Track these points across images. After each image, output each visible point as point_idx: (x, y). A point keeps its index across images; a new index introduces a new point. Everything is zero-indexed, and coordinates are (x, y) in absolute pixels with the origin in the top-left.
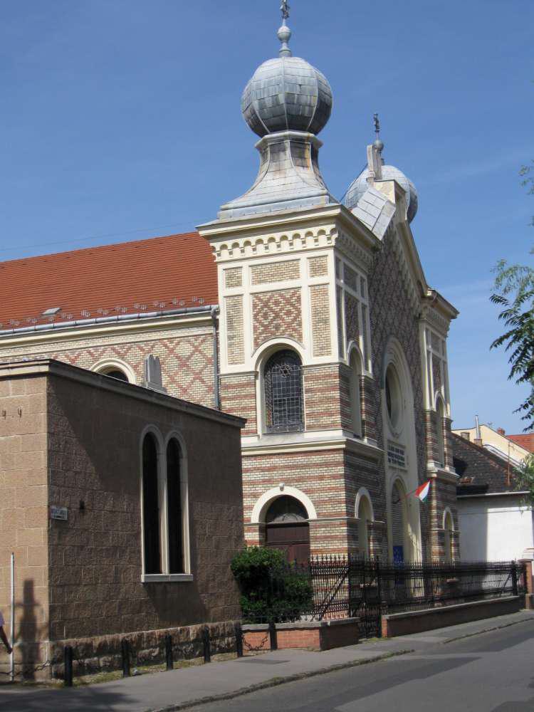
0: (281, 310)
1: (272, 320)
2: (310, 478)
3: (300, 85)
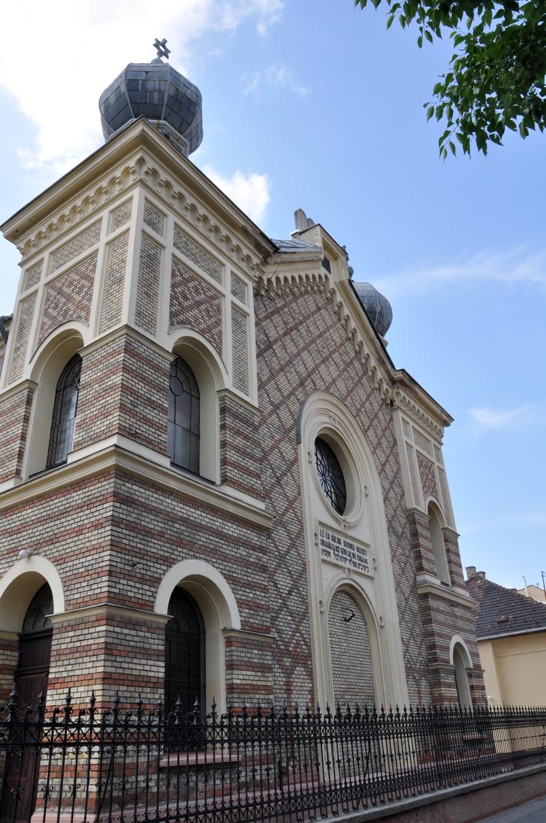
3: (147, 72)
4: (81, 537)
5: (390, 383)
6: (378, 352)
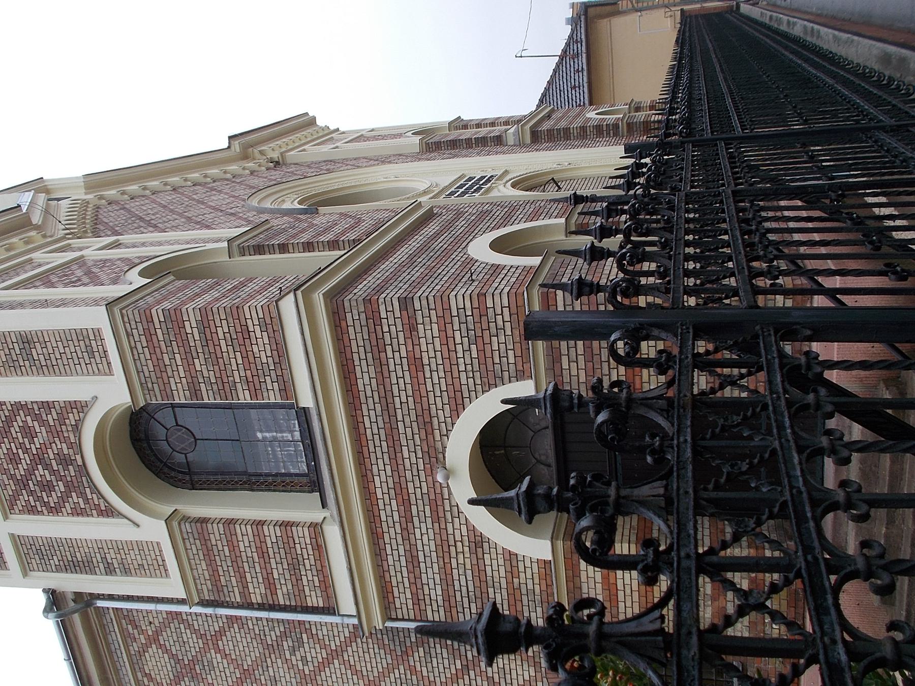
0: (26, 451)
1: (53, 472)
2: (419, 395)
4: (426, 361)
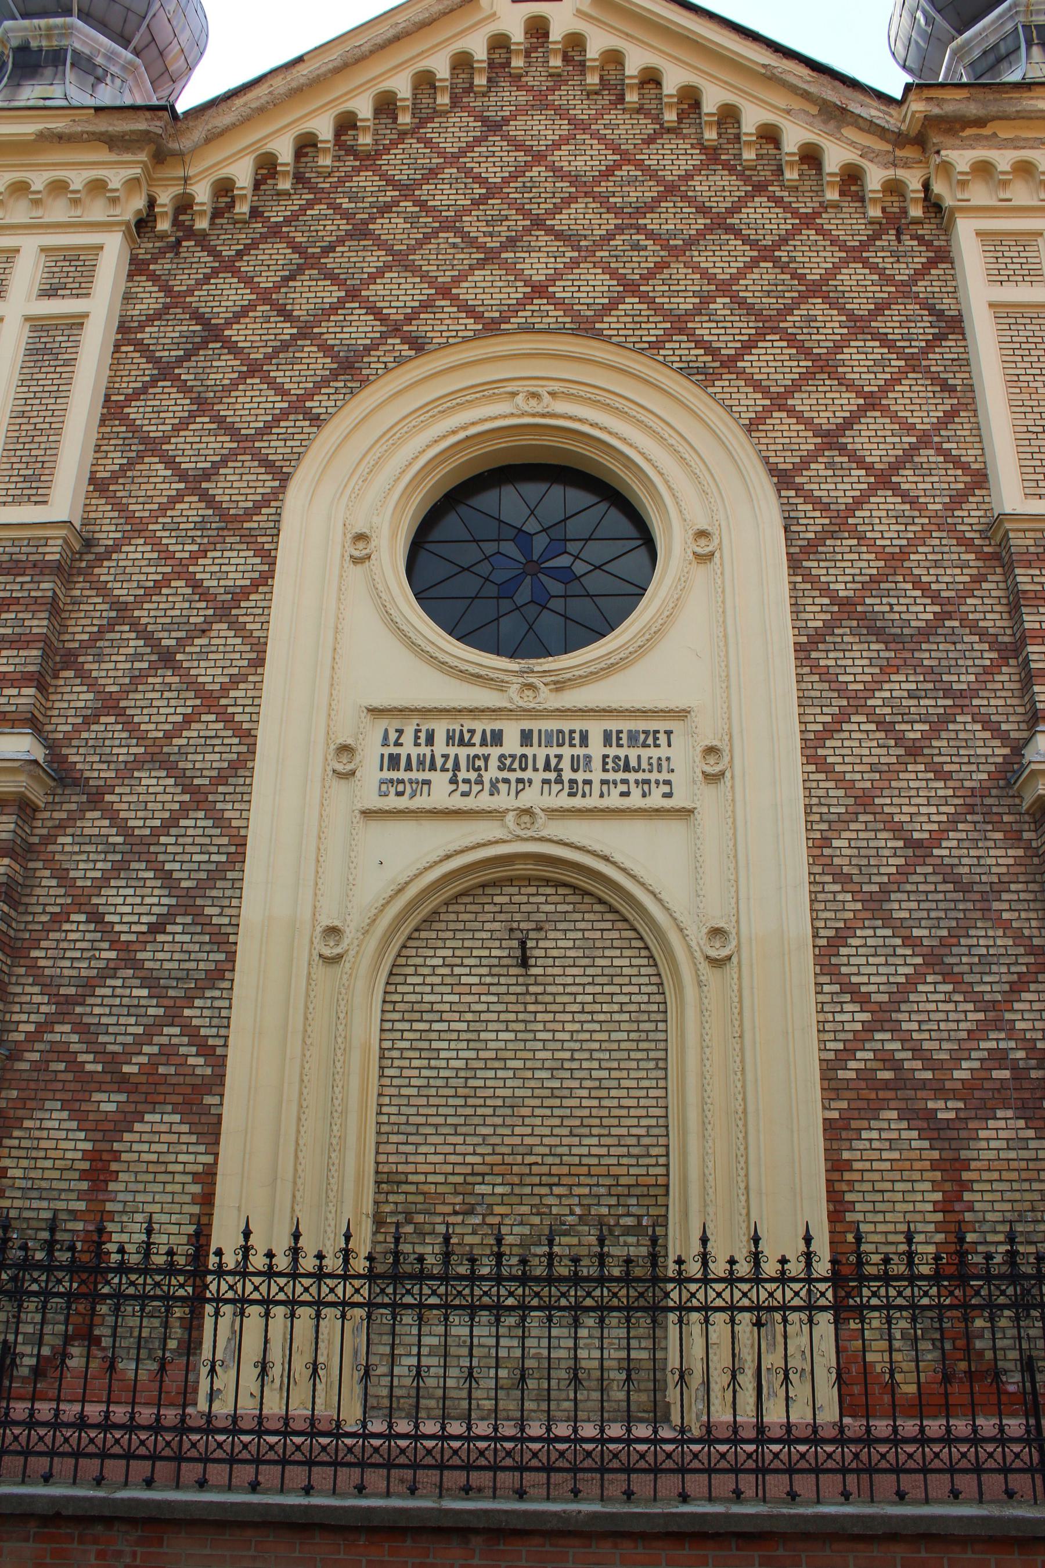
5: (908, 153)
6: (806, 95)
